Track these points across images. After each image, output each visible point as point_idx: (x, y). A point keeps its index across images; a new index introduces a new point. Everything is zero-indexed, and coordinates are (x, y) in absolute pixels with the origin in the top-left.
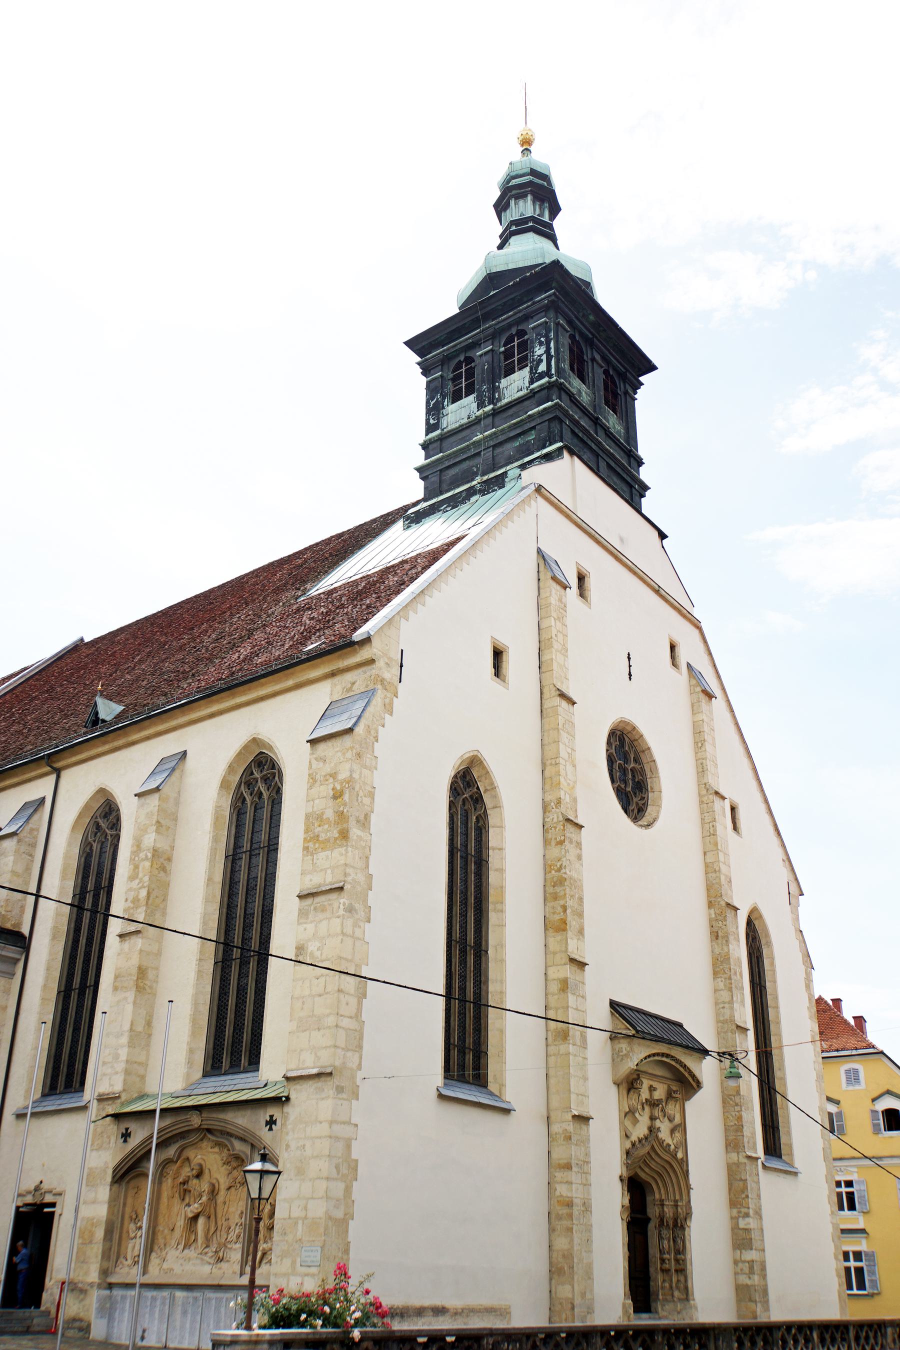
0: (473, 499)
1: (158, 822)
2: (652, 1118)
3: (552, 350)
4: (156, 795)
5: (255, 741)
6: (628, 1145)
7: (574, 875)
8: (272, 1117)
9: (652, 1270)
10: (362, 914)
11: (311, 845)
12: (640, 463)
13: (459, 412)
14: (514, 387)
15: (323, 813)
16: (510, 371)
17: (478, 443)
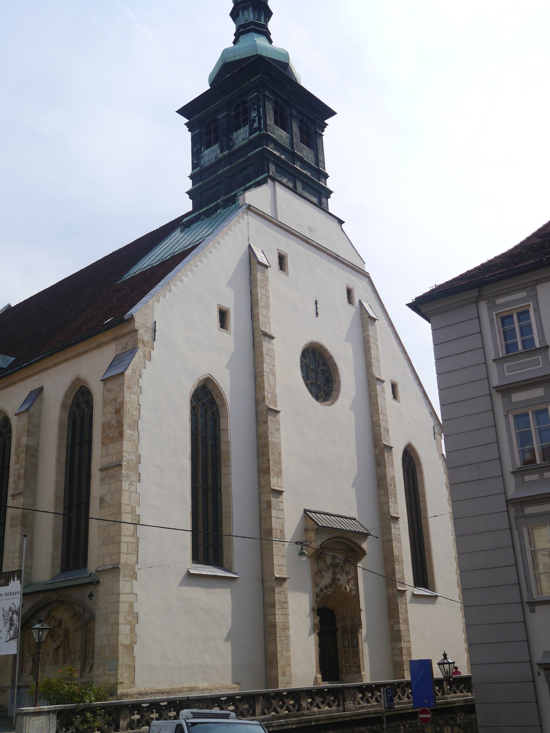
0: (219, 212)
1: (28, 430)
2: (335, 574)
3: (261, 113)
4: (26, 414)
5: (78, 380)
6: (318, 590)
7: (275, 440)
8: (91, 592)
9: (339, 657)
10: (134, 478)
11: (105, 440)
12: (326, 176)
13: (211, 154)
14: (241, 137)
15: (110, 422)
16: (238, 128)
17: (221, 174)
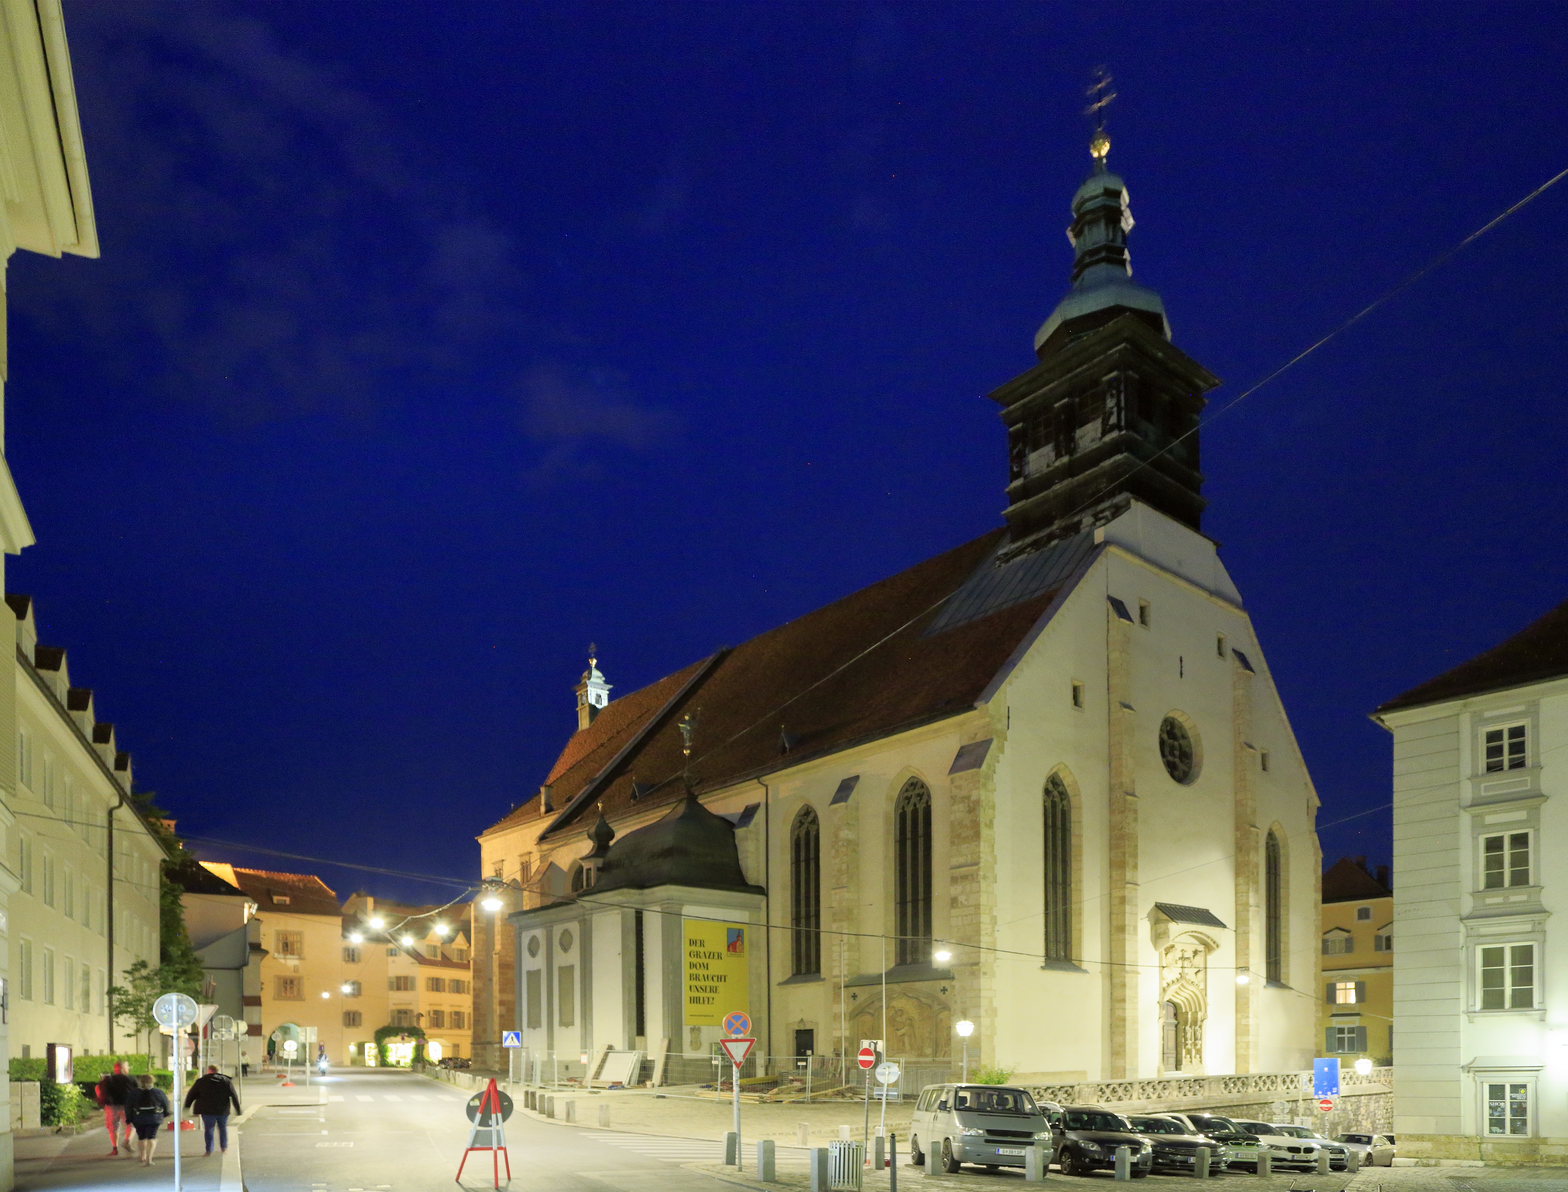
14: (1088, 439)
